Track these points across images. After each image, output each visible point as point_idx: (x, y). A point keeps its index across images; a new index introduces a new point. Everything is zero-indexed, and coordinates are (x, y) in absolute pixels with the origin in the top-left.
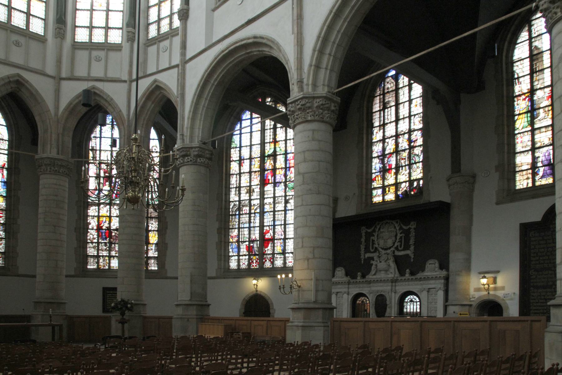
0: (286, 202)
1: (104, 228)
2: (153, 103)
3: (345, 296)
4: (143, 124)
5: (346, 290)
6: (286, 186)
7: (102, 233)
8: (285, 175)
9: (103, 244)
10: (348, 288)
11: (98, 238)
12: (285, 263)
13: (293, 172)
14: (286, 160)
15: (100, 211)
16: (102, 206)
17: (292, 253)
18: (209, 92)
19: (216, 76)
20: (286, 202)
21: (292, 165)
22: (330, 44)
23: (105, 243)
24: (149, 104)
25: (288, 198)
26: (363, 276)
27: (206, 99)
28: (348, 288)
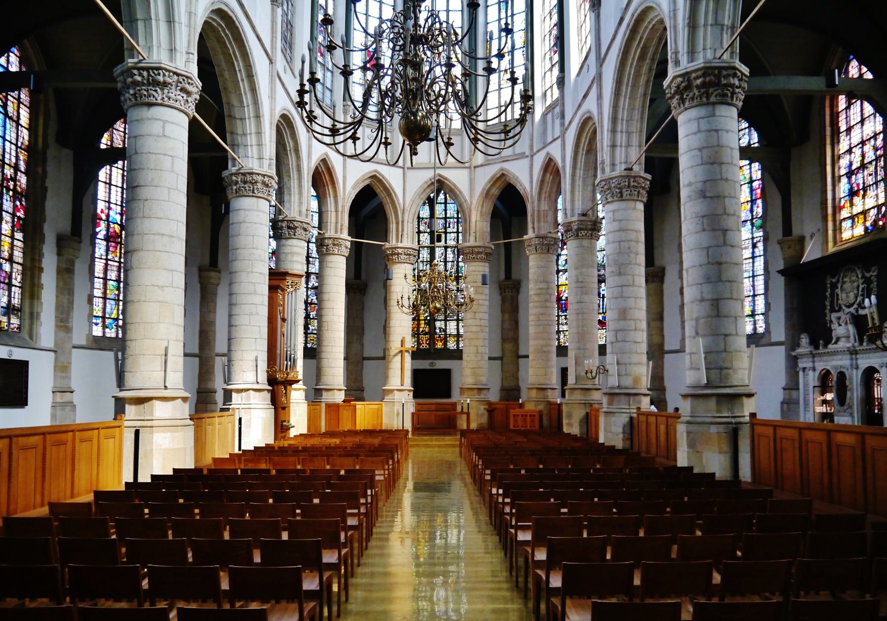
0: (754, 246)
1: (564, 298)
2: (550, 175)
3: (811, 373)
4: (545, 198)
5: (810, 365)
6: (752, 225)
7: (562, 304)
8: (752, 211)
9: (563, 317)
10: (814, 362)
11: (558, 310)
12: (755, 329)
13: (760, 205)
14: (752, 190)
15: (560, 280)
16: (561, 273)
17: (762, 314)
18: (581, 162)
19: (582, 145)
20: (754, 246)
21: (759, 196)
22: (620, 121)
23: (565, 316)
24: (548, 175)
25: (755, 241)
26: (826, 346)
27: (580, 169)
28: (814, 362)
